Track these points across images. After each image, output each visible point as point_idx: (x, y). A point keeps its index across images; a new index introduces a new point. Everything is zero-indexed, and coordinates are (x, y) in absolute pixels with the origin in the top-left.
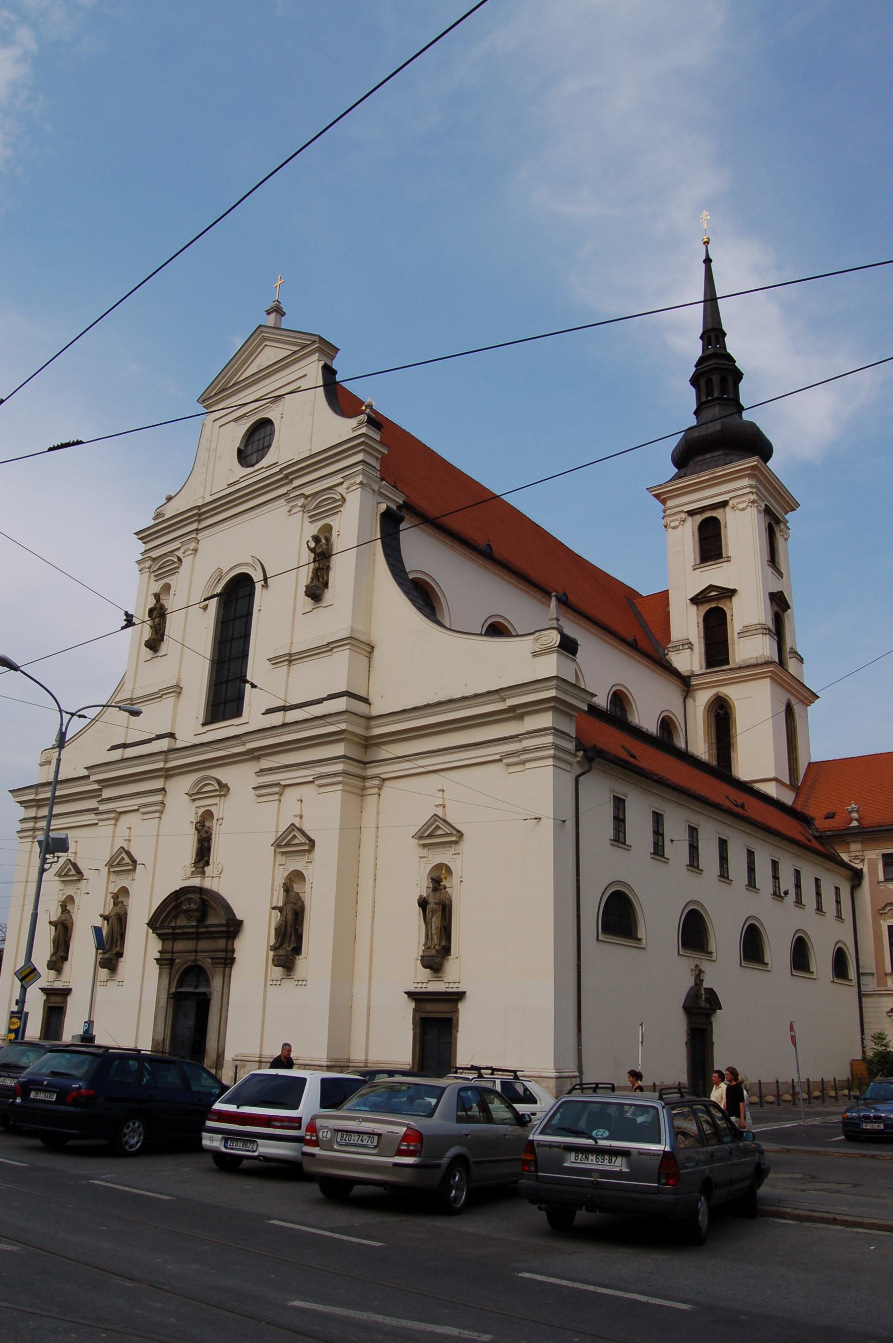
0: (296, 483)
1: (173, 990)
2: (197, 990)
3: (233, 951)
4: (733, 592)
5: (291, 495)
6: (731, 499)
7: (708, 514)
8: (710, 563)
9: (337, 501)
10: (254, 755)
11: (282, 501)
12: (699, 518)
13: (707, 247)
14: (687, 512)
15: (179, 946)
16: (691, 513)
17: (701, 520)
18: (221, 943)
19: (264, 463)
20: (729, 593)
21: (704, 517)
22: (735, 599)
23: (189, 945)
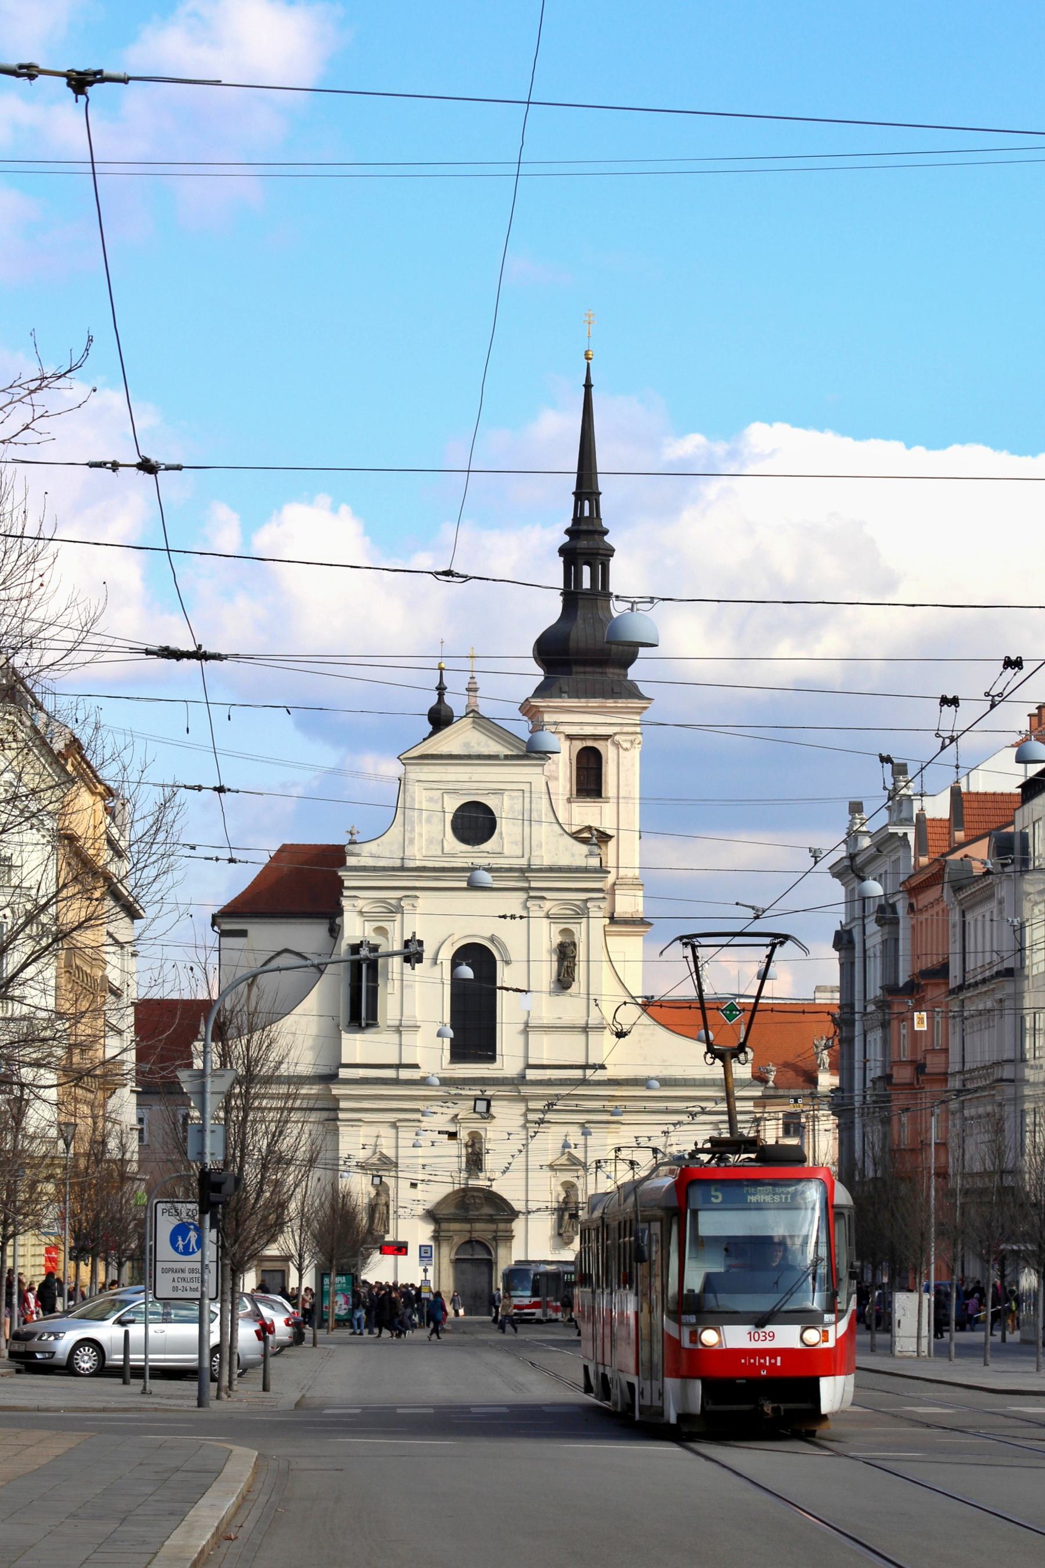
0: (533, 884)
1: (453, 1257)
2: (476, 1257)
3: (512, 1231)
4: (610, 837)
5: (532, 894)
6: (615, 734)
7: (590, 743)
8: (588, 800)
9: (579, 914)
10: (525, 1099)
11: (522, 895)
12: (579, 745)
13: (588, 364)
14: (568, 735)
15: (444, 1226)
16: (570, 737)
17: (580, 747)
18: (502, 1226)
19: (487, 846)
20: (604, 838)
21: (584, 745)
22: (609, 843)
23: (467, 1227)
